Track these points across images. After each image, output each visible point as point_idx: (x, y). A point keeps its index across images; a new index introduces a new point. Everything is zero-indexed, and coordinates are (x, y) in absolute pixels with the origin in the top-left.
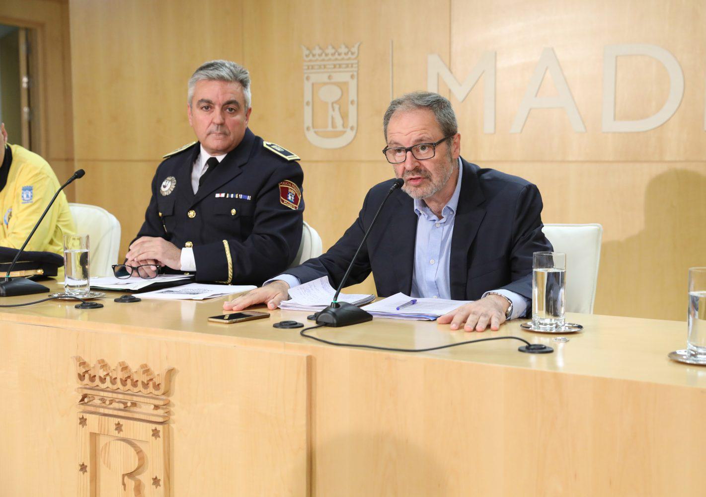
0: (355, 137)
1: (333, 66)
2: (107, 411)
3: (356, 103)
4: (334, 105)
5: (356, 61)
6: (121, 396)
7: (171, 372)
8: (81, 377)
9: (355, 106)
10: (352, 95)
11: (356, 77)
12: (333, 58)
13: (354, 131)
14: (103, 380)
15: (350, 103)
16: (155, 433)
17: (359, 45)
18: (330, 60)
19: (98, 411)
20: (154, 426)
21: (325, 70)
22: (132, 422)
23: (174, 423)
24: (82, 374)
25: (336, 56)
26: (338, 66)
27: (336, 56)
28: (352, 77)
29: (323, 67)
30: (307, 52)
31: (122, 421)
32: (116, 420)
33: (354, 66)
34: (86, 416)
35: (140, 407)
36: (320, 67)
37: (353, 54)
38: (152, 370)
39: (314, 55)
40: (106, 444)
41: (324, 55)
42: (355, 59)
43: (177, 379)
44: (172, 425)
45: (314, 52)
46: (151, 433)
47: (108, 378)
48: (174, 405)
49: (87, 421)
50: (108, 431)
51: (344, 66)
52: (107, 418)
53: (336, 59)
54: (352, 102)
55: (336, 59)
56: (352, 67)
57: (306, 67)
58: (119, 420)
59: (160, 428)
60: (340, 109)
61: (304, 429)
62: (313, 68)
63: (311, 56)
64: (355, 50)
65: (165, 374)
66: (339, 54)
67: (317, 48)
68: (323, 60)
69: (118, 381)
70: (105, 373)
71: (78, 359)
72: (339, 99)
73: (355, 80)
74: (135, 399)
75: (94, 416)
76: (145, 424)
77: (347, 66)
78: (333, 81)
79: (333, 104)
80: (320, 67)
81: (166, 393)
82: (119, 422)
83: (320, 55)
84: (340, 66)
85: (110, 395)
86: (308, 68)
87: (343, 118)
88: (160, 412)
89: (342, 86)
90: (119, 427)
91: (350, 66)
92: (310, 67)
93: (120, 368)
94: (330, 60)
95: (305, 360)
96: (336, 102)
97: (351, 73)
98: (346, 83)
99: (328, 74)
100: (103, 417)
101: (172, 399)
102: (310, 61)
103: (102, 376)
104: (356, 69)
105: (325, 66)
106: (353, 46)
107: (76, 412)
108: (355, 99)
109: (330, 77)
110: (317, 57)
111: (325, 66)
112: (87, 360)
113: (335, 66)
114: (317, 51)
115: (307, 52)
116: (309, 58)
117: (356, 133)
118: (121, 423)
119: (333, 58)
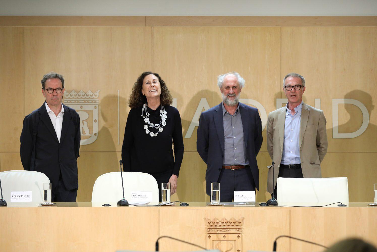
0: (97, 138)
1: (83, 102)
2: (219, 233)
3: (97, 121)
4: (84, 122)
5: (97, 100)
6: (225, 227)
7: (243, 219)
8: (208, 223)
9: (97, 123)
10: (96, 117)
11: (98, 107)
12: (83, 97)
13: (97, 136)
14: (217, 223)
15: (94, 121)
16: (239, 236)
17: (99, 91)
18: (81, 98)
19: (216, 233)
20: (238, 235)
21: (79, 104)
22: (229, 235)
23: (243, 233)
24: (209, 222)
25: (85, 96)
26: (86, 102)
27: (85, 96)
28: (95, 107)
29: (77, 102)
30: (67, 94)
31: (225, 235)
32: (223, 235)
33: (96, 102)
34: (211, 235)
35: (230, 230)
36: (75, 102)
37: (95, 95)
38: (235, 219)
39: (71, 96)
40: (219, 242)
41: (77, 95)
42: (97, 98)
43: (244, 220)
44: (242, 234)
45: (71, 94)
46: (237, 237)
47: (220, 223)
48: (243, 228)
49: (211, 237)
50: (220, 239)
51: (91, 102)
52: (219, 235)
53: (85, 98)
54: (95, 121)
55: (85, 98)
56: (95, 102)
57: (67, 102)
58: (224, 235)
59: (240, 235)
60: (87, 124)
61: (289, 229)
62: (70, 102)
63: (69, 95)
64: (97, 93)
65: (242, 219)
66: (87, 96)
67: (73, 92)
68: (77, 98)
69: (224, 223)
70: (219, 221)
71: (208, 219)
72: (87, 119)
73: (97, 109)
74: (231, 228)
75: (214, 235)
76: (234, 235)
77: (92, 102)
78: (82, 109)
79: (83, 121)
80: (75, 102)
81: (241, 226)
82: (224, 235)
83: (75, 95)
84: (88, 102)
85: (221, 227)
86: (68, 102)
87: (89, 129)
88: (240, 230)
89: (90, 112)
90: (224, 236)
91: (94, 102)
92: (69, 102)
93: (225, 220)
94: (81, 98)
95: (289, 211)
96: (84, 120)
97: (95, 106)
98: (92, 111)
99: (81, 106)
100: (218, 235)
101: (242, 227)
102: (69, 98)
103: (218, 222)
104: (98, 104)
105: (78, 102)
106: (96, 92)
107: (204, 235)
108: (97, 119)
109: (81, 107)
110: (73, 96)
111: (78, 102)
112: (209, 218)
113: (84, 102)
114: (73, 93)
115: (67, 94)
116: (67, 97)
117: (98, 137)
118: (225, 236)
119: (83, 97)
